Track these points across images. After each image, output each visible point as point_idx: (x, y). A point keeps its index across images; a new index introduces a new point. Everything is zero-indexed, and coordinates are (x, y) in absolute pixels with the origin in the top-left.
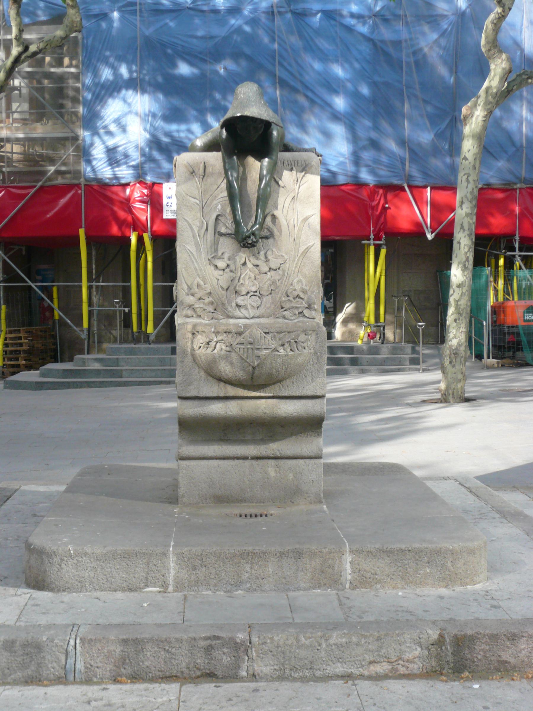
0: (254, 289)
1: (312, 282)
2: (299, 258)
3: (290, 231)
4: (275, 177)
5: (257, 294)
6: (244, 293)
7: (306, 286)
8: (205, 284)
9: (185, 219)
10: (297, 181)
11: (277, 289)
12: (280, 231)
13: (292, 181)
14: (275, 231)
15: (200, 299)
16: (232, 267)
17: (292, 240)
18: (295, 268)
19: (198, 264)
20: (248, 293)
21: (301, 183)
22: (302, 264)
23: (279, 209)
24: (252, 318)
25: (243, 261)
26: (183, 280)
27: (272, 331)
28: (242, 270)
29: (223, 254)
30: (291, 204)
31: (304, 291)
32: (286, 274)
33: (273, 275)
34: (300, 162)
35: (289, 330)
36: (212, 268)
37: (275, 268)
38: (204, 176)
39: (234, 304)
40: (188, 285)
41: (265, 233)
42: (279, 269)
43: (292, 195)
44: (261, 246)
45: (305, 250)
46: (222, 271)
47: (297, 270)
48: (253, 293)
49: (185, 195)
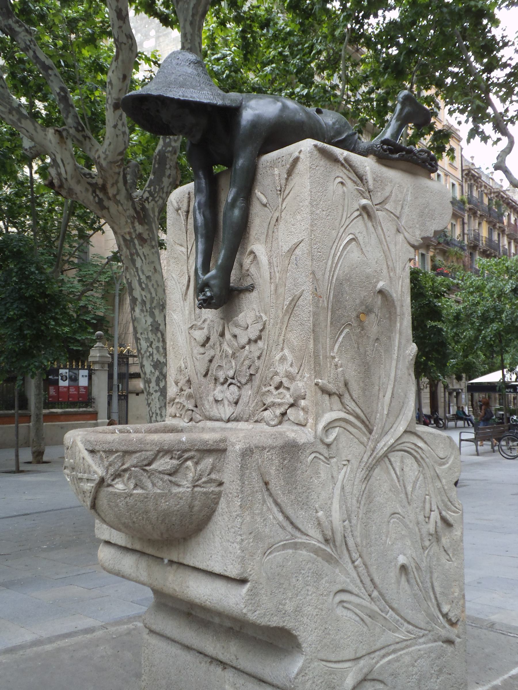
0: (231, 373)
2: (283, 317)
7: (291, 365)
18: (279, 336)
20: (226, 380)
24: (229, 421)
25: (220, 329)
27: (97, 448)
29: (204, 321)
31: (291, 377)
35: (124, 448)
39: (211, 399)
41: (247, 283)
45: (290, 304)
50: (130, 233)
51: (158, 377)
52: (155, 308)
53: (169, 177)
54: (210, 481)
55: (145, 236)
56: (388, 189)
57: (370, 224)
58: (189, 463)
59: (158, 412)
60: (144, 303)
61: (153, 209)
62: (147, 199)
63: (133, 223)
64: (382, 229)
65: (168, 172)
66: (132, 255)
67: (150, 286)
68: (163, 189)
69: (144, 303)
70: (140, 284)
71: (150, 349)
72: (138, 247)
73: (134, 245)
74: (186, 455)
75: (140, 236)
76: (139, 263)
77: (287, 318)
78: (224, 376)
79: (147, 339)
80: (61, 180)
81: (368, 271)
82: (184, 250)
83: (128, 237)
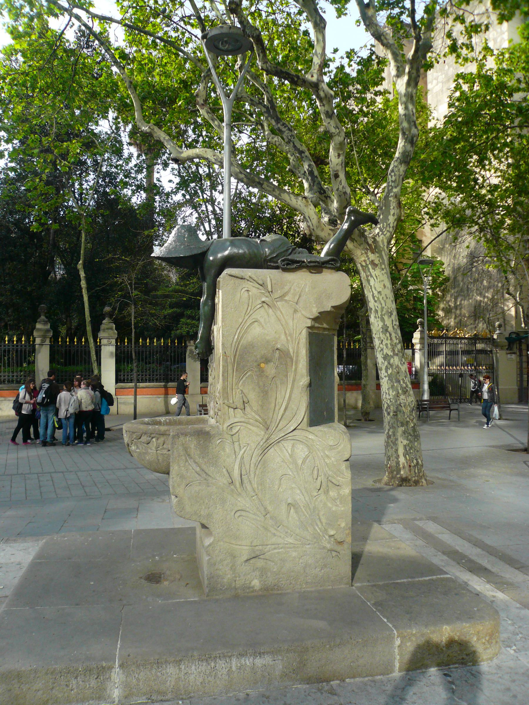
50: (365, 261)
51: (387, 366)
52: (384, 315)
53: (394, 215)
54: (164, 449)
55: (377, 262)
56: (286, 288)
57: (270, 311)
58: (154, 439)
59: (387, 392)
60: (376, 311)
61: (382, 241)
62: (378, 233)
63: (366, 253)
64: (281, 312)
65: (392, 212)
66: (367, 276)
67: (381, 299)
68: (389, 224)
69: (376, 311)
70: (374, 297)
71: (381, 346)
72: (371, 270)
73: (369, 269)
74: (152, 435)
75: (372, 262)
76: (372, 282)
79: (379, 338)
80: (310, 230)
81: (268, 338)
83: (364, 264)
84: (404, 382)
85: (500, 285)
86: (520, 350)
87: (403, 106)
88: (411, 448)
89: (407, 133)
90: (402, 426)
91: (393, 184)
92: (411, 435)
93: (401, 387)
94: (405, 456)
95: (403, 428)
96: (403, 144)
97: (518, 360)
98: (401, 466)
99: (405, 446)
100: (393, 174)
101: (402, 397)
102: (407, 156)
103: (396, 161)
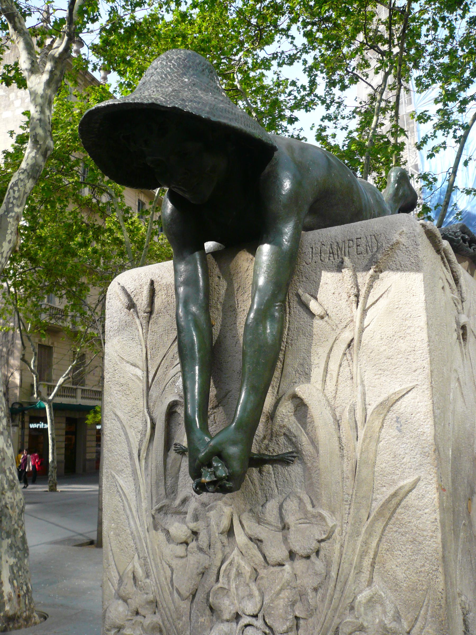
1: (419, 607)
2: (372, 525)
3: (344, 440)
4: (300, 292)
5: (259, 623)
6: (226, 616)
8: (148, 576)
9: (116, 415)
10: (357, 296)
11: (311, 615)
12: (314, 442)
13: (345, 296)
14: (304, 440)
15: (137, 613)
16: (203, 538)
17: (347, 467)
19: (135, 523)
20: (237, 617)
21: (370, 301)
22: (384, 546)
23: (312, 379)
25: (225, 523)
26: (111, 558)
28: (228, 550)
29: (185, 501)
30: (345, 363)
32: (333, 574)
33: (299, 573)
34: (363, 241)
36: (161, 536)
37: (303, 552)
38: (151, 313)
40: (119, 573)
42: (317, 553)
43: (346, 336)
44: (273, 485)
45: (388, 501)
46: (183, 547)
47: (367, 562)
48: (245, 620)
49: (117, 359)
53: (9, 242)
65: (8, 237)
77: (379, 526)
78: (233, 610)
82: (140, 373)
84: (11, 473)
85: (5, 350)
86: (23, 423)
87: (38, 109)
88: (19, 569)
89: (41, 142)
90: (8, 537)
91: (15, 202)
92: (20, 550)
93: (8, 480)
94: (11, 582)
95: (9, 541)
96: (33, 154)
97: (20, 434)
98: (6, 598)
99: (12, 567)
100: (16, 188)
101: (9, 494)
102: (38, 171)
103: (23, 173)
